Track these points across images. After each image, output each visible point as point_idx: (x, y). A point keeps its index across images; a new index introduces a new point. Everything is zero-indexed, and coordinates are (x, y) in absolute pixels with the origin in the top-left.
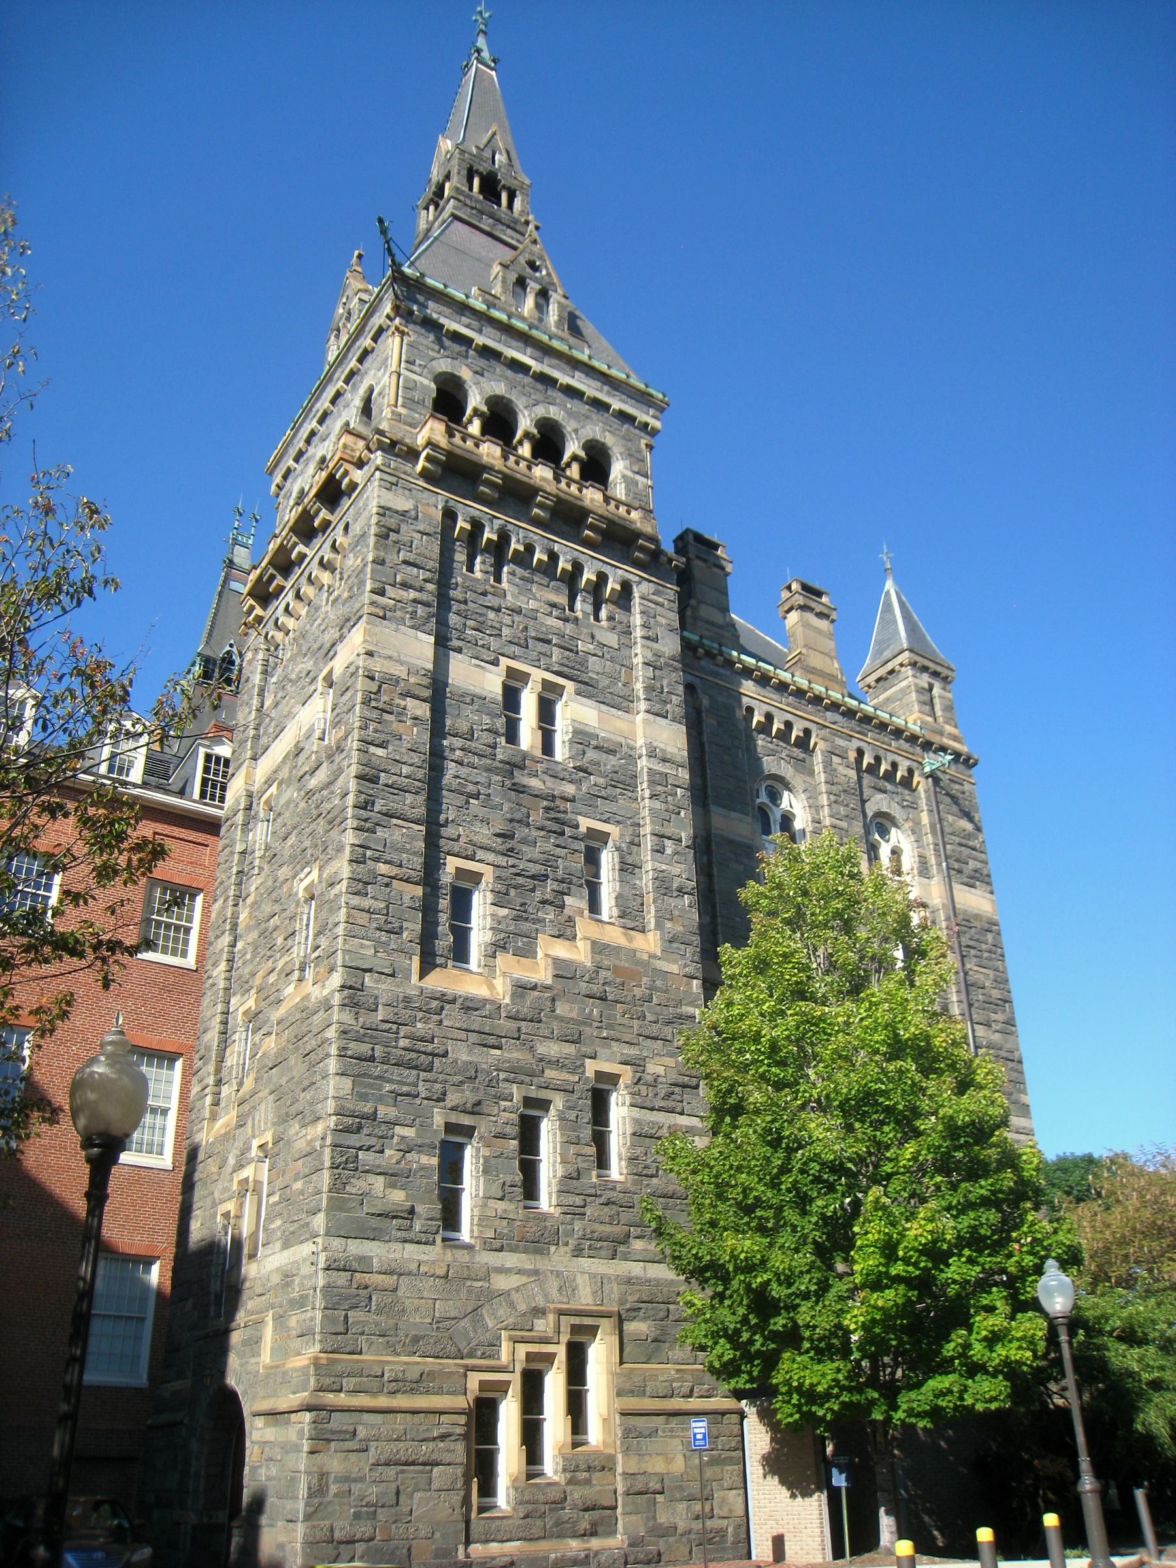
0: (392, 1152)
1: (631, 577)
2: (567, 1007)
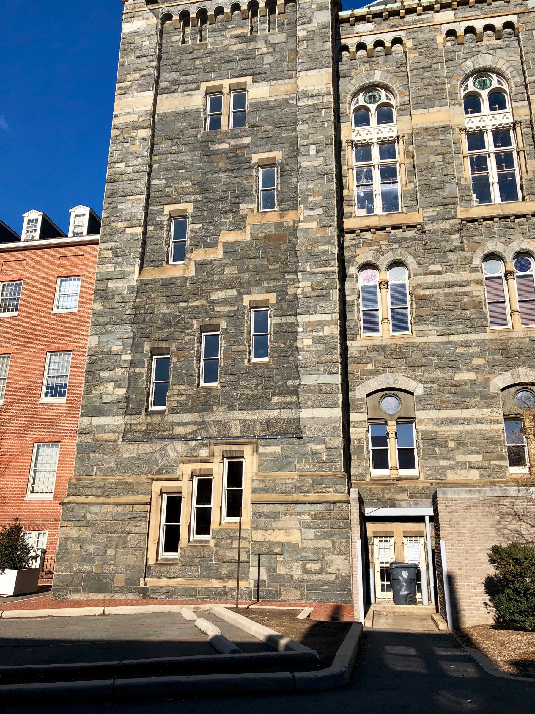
0: (119, 369)
2: (233, 268)
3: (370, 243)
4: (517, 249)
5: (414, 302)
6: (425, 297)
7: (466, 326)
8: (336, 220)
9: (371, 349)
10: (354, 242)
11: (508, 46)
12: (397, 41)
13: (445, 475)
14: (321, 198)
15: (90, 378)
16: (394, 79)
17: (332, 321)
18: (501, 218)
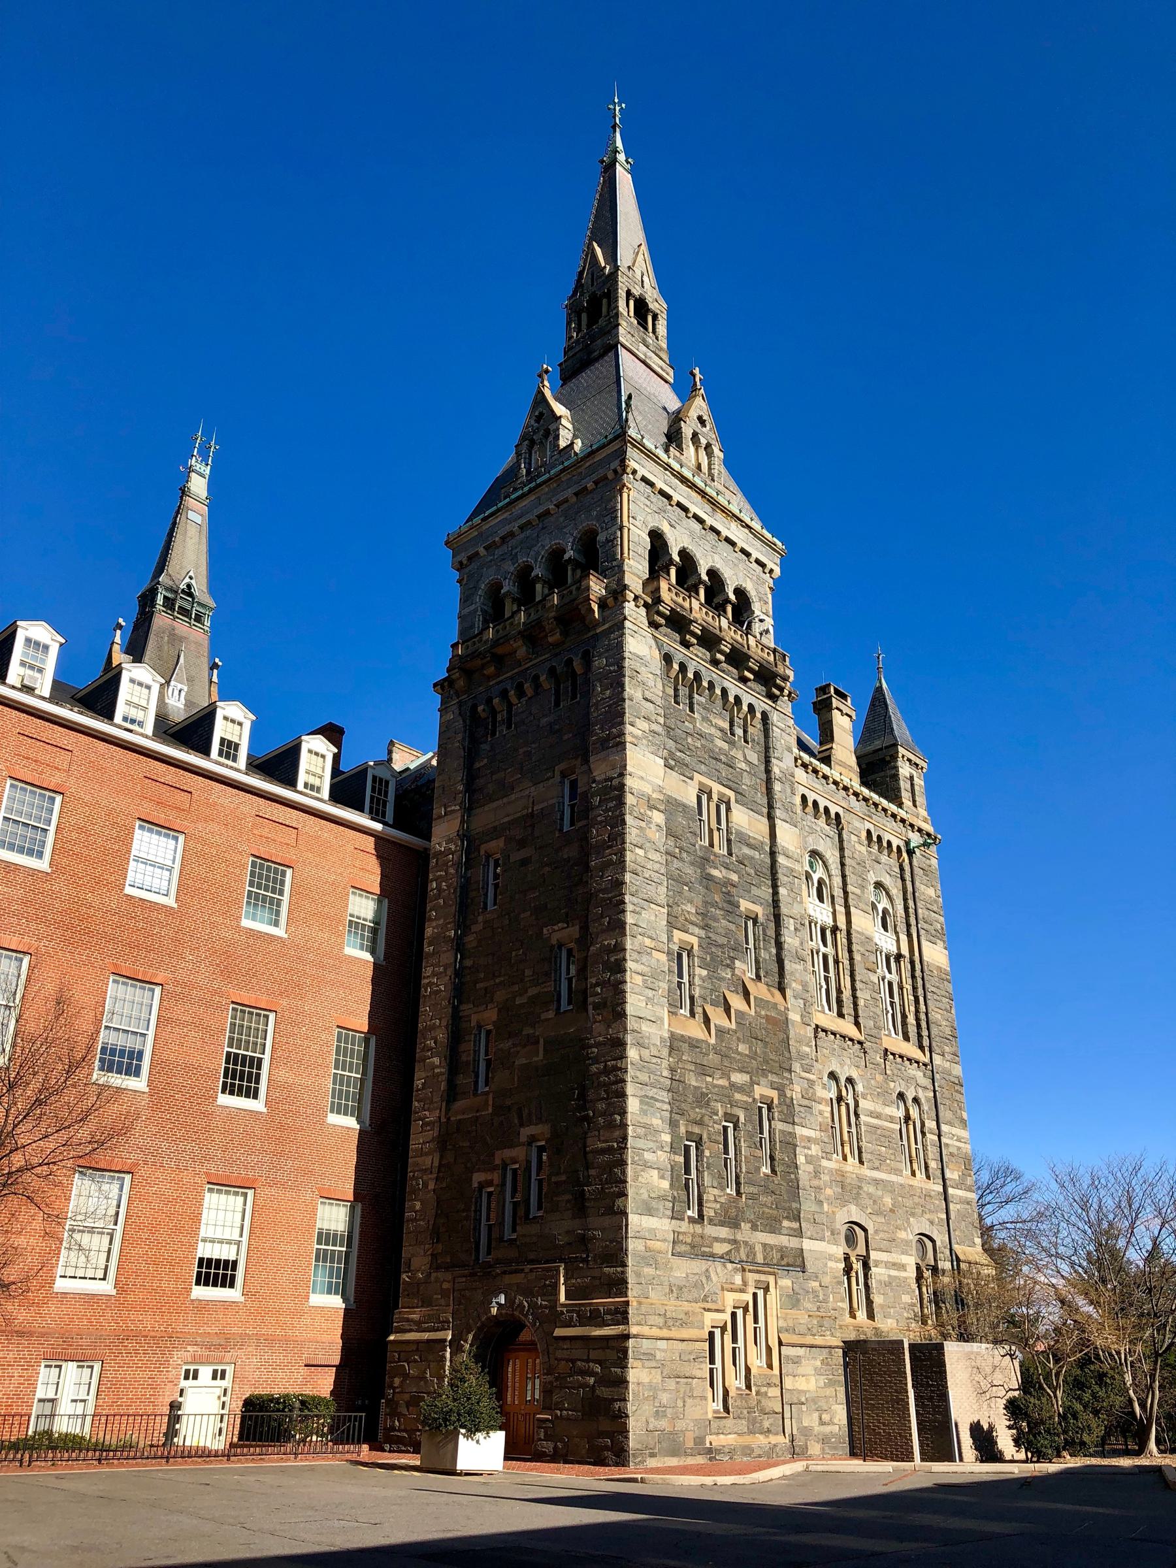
1: (767, 707)
15: (636, 1158)
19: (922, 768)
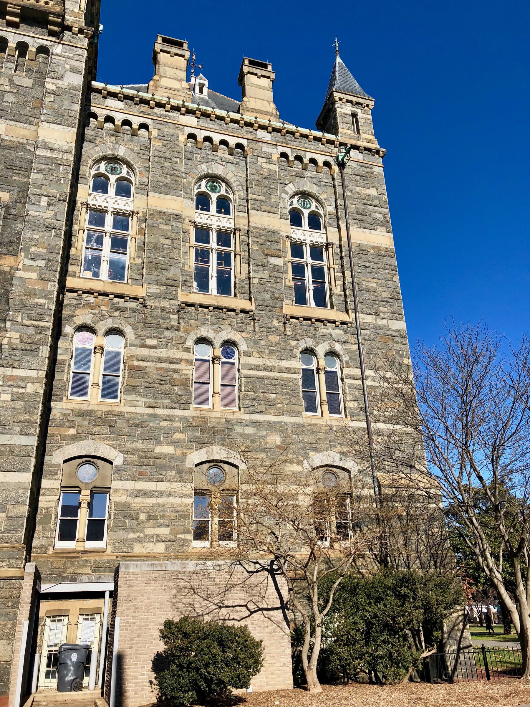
3: (91, 306)
4: (225, 338)
5: (126, 371)
6: (138, 368)
7: (172, 401)
8: (58, 275)
9: (76, 413)
10: (75, 302)
11: (237, 164)
12: (143, 126)
13: (132, 548)
14: (45, 251)
16: (137, 159)
17: (37, 378)
18: (215, 308)
19: (368, 106)
